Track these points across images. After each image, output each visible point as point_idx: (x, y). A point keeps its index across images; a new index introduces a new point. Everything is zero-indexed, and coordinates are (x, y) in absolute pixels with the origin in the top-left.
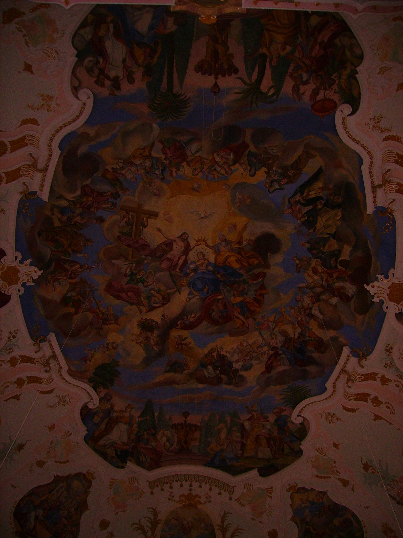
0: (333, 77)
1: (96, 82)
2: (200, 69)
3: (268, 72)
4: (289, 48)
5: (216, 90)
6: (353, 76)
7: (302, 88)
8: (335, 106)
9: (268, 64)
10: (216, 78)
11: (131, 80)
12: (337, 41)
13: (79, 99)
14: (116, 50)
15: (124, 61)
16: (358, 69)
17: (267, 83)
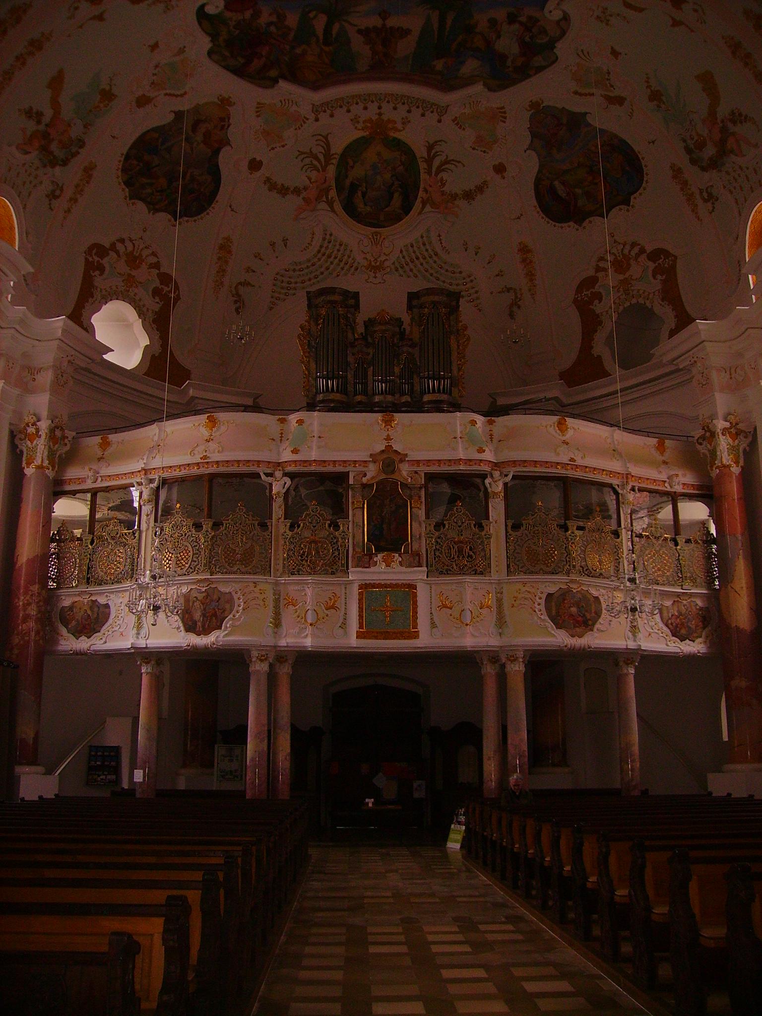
0: (237, 32)
1: (539, 21)
2: (405, 33)
3: (320, 32)
4: (298, 51)
5: (384, 15)
6: (214, 37)
7: (274, 19)
8: (226, 7)
9: (321, 37)
10: (384, 25)
11: (493, 22)
12: (242, 61)
13: (564, 12)
14: (507, 44)
15: (499, 37)
16: (210, 45)
17: (320, 23)
